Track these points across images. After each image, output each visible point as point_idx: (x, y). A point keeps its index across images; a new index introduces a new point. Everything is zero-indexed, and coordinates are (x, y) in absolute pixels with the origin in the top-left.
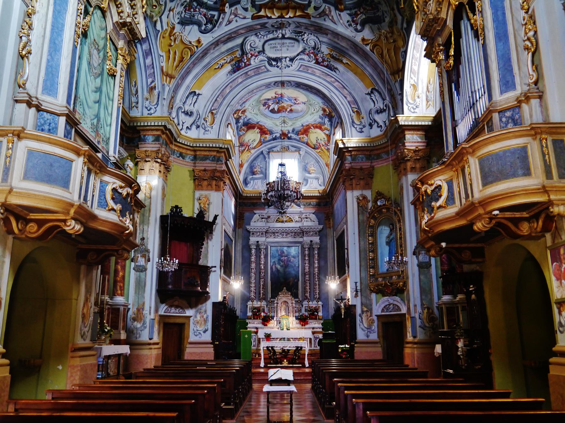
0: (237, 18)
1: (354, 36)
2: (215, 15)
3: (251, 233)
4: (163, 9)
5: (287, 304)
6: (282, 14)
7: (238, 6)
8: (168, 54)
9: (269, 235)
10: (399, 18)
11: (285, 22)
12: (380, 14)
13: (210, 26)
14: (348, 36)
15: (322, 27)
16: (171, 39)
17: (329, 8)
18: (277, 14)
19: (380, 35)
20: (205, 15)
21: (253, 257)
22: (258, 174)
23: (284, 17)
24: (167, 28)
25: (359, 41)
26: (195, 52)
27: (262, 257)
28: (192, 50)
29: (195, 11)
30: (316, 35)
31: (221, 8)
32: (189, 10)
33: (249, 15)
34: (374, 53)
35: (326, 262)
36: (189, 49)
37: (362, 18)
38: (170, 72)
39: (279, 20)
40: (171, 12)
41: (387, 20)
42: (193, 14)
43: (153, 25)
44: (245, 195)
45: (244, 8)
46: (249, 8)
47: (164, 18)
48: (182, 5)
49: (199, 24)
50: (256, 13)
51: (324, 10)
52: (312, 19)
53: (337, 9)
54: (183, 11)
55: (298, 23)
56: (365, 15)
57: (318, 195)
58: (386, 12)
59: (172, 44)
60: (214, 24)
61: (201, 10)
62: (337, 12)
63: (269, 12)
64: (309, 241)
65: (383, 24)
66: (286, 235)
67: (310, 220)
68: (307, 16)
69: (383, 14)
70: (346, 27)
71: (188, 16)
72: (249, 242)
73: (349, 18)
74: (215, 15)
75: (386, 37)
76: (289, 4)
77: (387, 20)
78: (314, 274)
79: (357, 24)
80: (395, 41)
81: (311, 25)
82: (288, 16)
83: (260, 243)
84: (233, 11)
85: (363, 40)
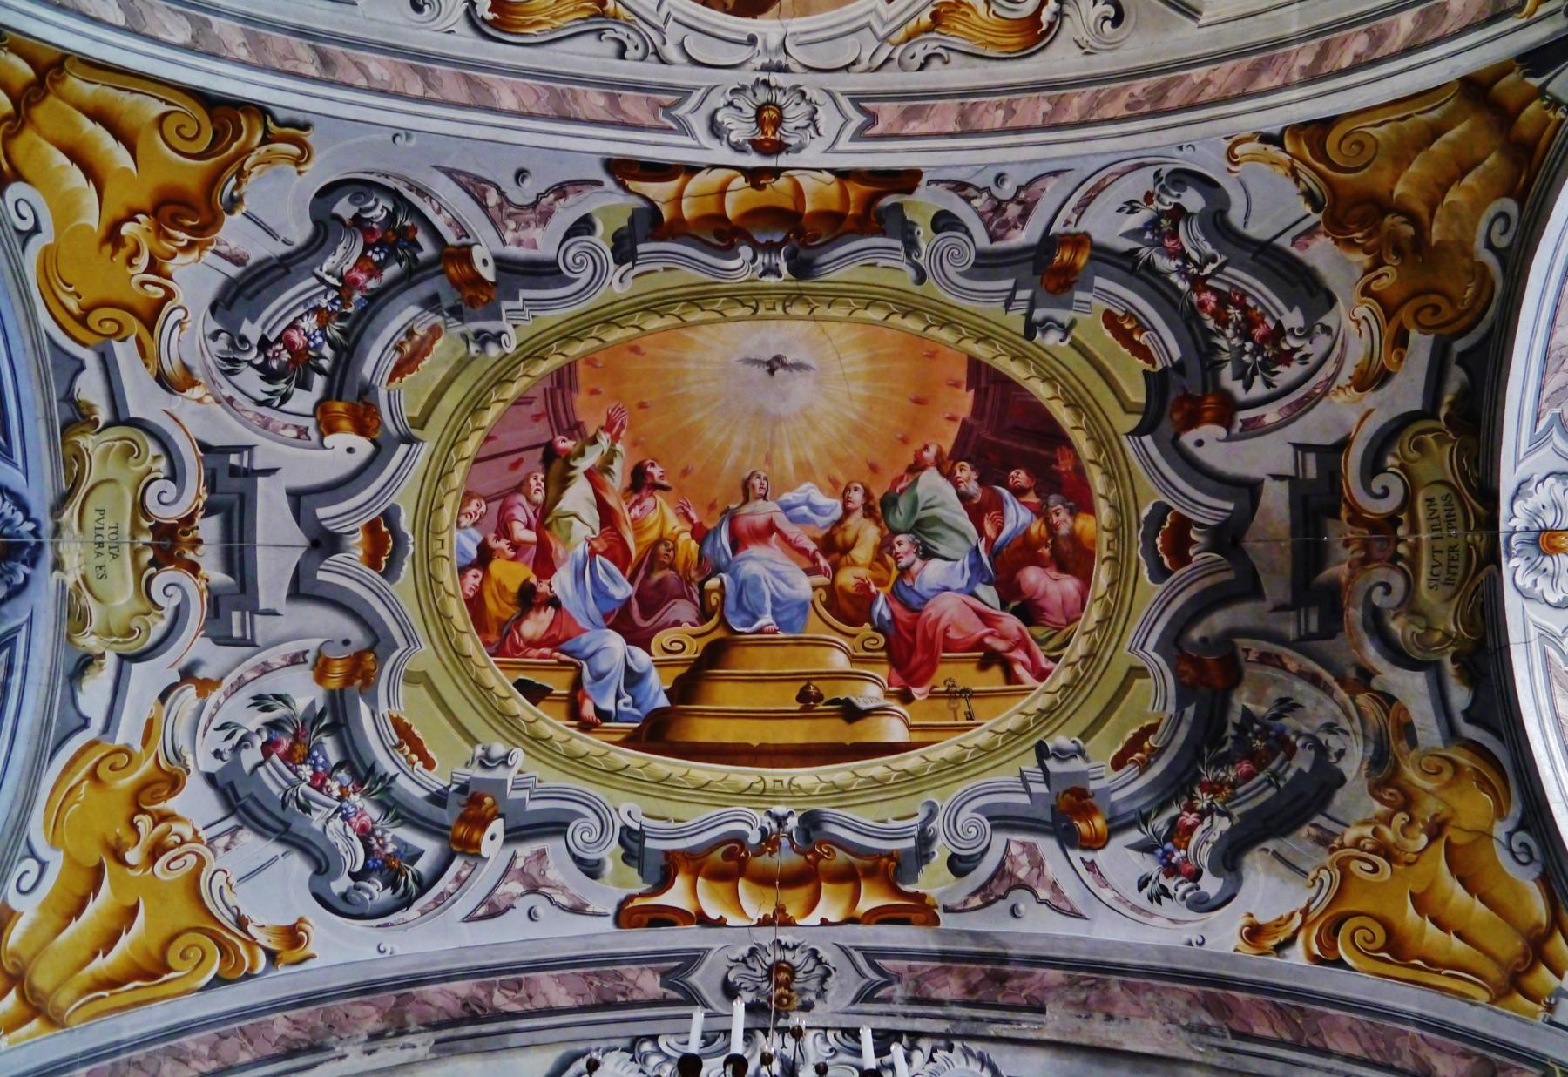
0: (533, 900)
1: (1195, 938)
2: (417, 855)
4: (155, 634)
6: (780, 909)
7: (553, 846)
8: (80, 885)
10: (1411, 688)
11: (796, 958)
12: (1303, 761)
13: (377, 892)
14: (1165, 951)
15: (1003, 959)
16: (133, 827)
17: (1030, 850)
18: (755, 912)
19: (1343, 865)
20: (365, 834)
23: (788, 922)
24: (138, 747)
25: (1230, 950)
26: (249, 976)
28: (239, 958)
29: (318, 782)
30: (976, 1047)
31: (461, 830)
32: (287, 757)
33: (605, 896)
34: (1340, 963)
36: (219, 945)
37: (1214, 838)
38: (43, 979)
39: (766, 936)
40: (191, 691)
41: (1353, 763)
42: (307, 797)
43: (67, 663)
45: (579, 861)
46: (609, 866)
47: (146, 679)
48: (261, 703)
49: (323, 864)
50: (642, 895)
51: (1002, 864)
52: (947, 921)
53: (1068, 839)
54: (258, 742)
55: (872, 956)
56: (1222, 814)
58: (1330, 728)
59: (133, 856)
60: (407, 891)
61: (355, 798)
62: (1075, 855)
63: (714, 895)
65: (1340, 798)
68: (920, 911)
69: (1321, 750)
70: (1141, 911)
71: (275, 790)
73: (1149, 865)
74: (420, 854)
75: (1387, 852)
76: (820, 857)
77: (1353, 763)
79: (1196, 875)
80: (1436, 830)
81: (944, 956)
82: (814, 919)
84: (519, 863)
85: (1254, 933)
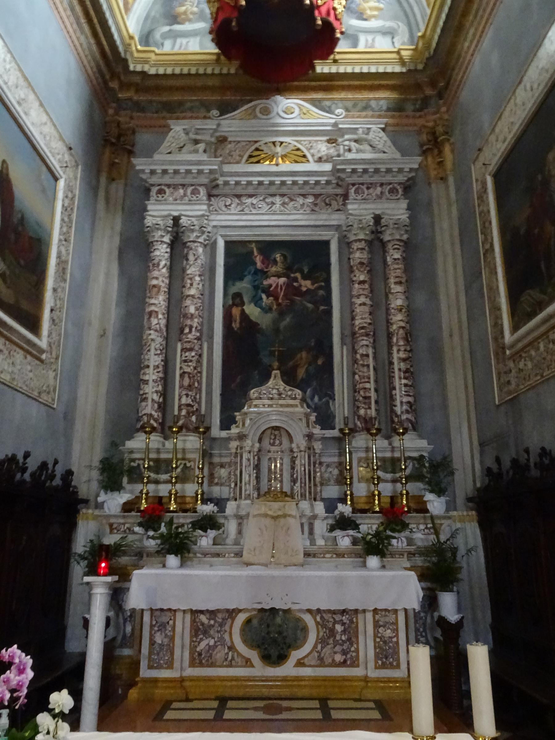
3: (154, 190)
5: (285, 441)
9: (221, 204)
21: (156, 273)
22: (190, 21)
27: (192, 270)
35: (434, 295)
44: (139, 68)
57: (398, 69)
64: (369, 219)
66: (284, 204)
67: (368, 148)
72: (144, 218)
78: (390, 336)
83: (184, 221)
